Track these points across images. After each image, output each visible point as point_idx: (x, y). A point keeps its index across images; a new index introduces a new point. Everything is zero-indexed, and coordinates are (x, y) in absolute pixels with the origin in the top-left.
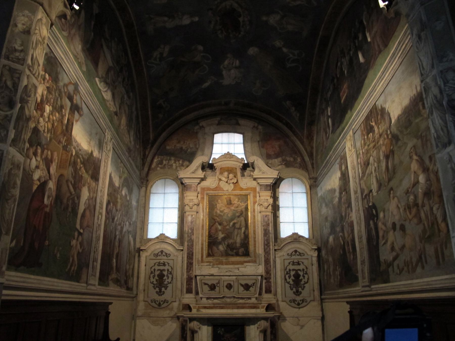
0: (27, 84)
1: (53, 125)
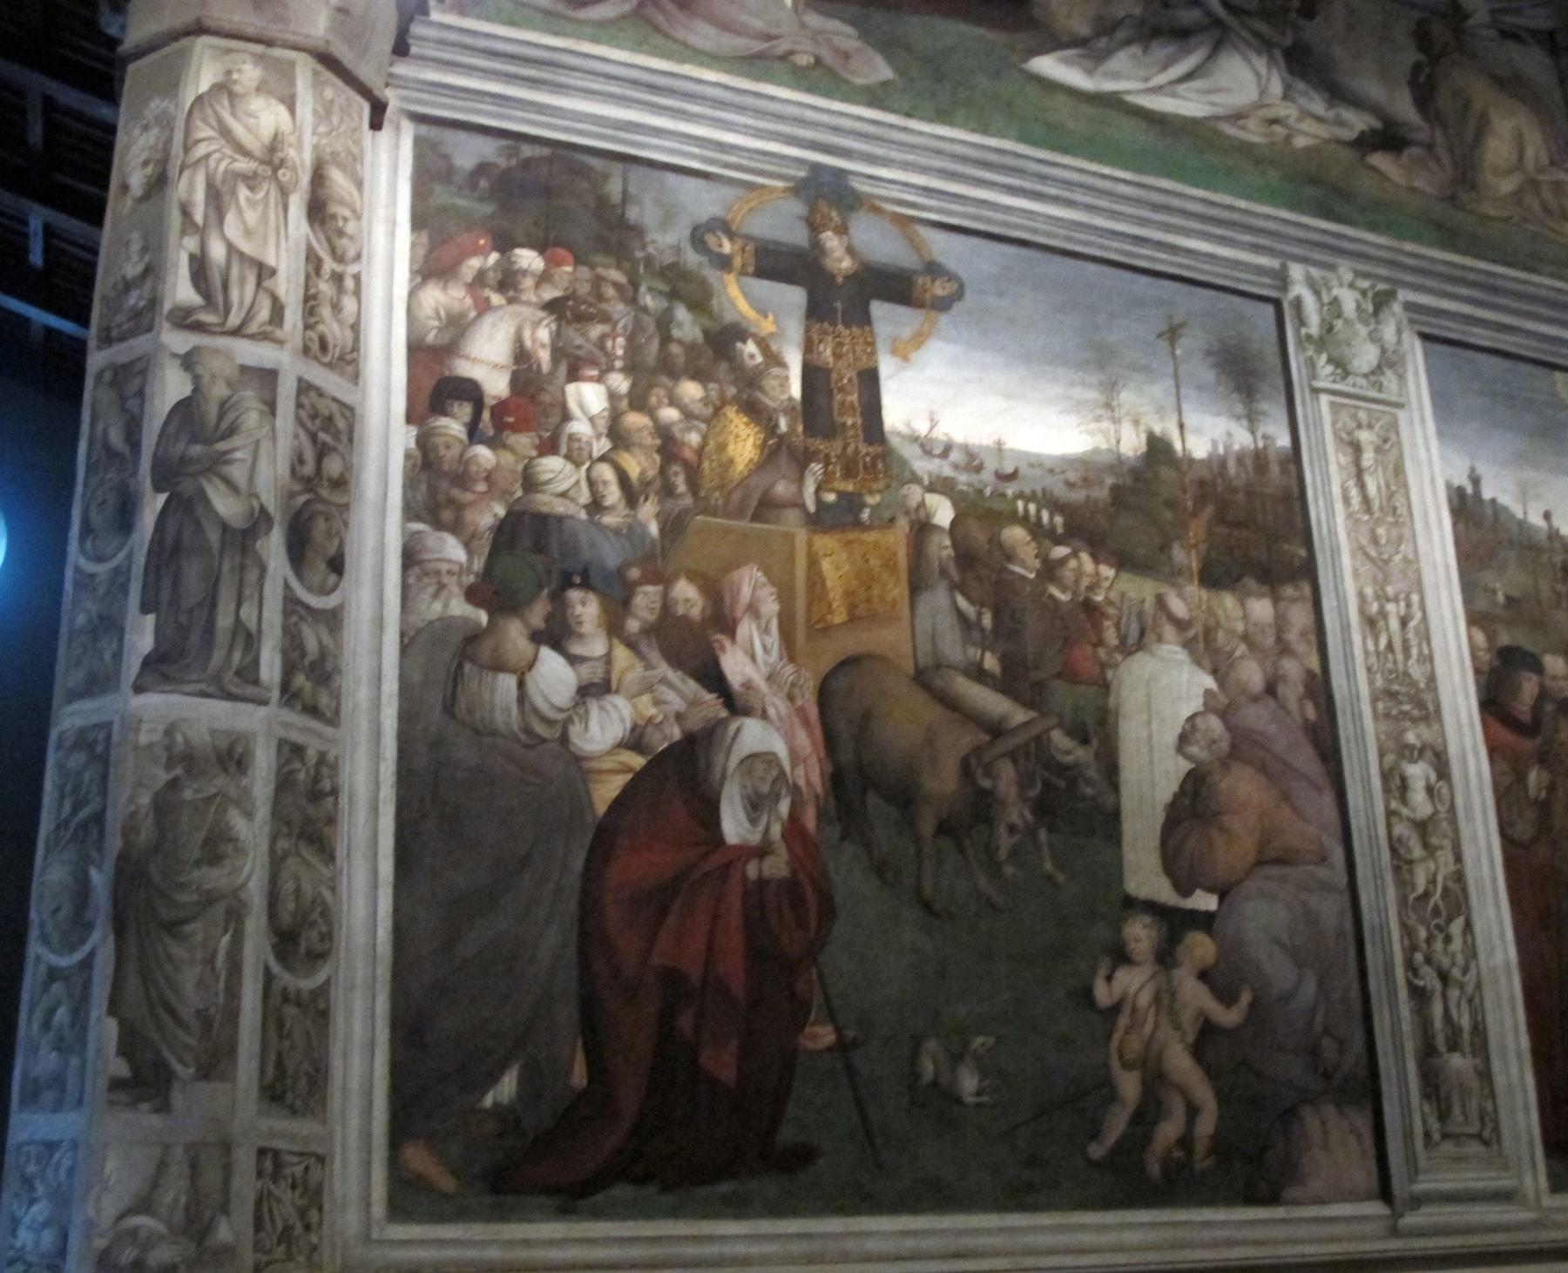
0: (197, 389)
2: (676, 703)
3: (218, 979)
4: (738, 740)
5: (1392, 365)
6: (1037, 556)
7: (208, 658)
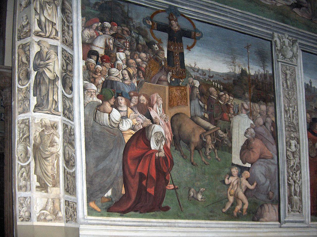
1: (139, 68)
2: (141, 121)
3: (55, 169)
4: (154, 128)
5: (295, 57)
6: (217, 94)
7: (48, 106)
